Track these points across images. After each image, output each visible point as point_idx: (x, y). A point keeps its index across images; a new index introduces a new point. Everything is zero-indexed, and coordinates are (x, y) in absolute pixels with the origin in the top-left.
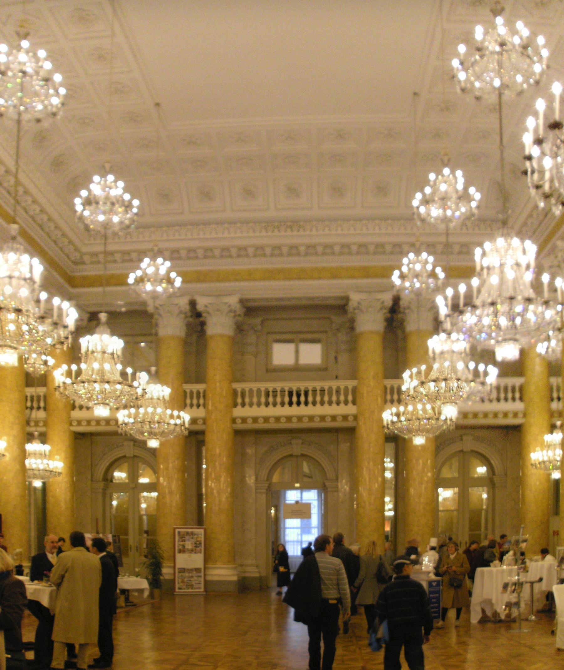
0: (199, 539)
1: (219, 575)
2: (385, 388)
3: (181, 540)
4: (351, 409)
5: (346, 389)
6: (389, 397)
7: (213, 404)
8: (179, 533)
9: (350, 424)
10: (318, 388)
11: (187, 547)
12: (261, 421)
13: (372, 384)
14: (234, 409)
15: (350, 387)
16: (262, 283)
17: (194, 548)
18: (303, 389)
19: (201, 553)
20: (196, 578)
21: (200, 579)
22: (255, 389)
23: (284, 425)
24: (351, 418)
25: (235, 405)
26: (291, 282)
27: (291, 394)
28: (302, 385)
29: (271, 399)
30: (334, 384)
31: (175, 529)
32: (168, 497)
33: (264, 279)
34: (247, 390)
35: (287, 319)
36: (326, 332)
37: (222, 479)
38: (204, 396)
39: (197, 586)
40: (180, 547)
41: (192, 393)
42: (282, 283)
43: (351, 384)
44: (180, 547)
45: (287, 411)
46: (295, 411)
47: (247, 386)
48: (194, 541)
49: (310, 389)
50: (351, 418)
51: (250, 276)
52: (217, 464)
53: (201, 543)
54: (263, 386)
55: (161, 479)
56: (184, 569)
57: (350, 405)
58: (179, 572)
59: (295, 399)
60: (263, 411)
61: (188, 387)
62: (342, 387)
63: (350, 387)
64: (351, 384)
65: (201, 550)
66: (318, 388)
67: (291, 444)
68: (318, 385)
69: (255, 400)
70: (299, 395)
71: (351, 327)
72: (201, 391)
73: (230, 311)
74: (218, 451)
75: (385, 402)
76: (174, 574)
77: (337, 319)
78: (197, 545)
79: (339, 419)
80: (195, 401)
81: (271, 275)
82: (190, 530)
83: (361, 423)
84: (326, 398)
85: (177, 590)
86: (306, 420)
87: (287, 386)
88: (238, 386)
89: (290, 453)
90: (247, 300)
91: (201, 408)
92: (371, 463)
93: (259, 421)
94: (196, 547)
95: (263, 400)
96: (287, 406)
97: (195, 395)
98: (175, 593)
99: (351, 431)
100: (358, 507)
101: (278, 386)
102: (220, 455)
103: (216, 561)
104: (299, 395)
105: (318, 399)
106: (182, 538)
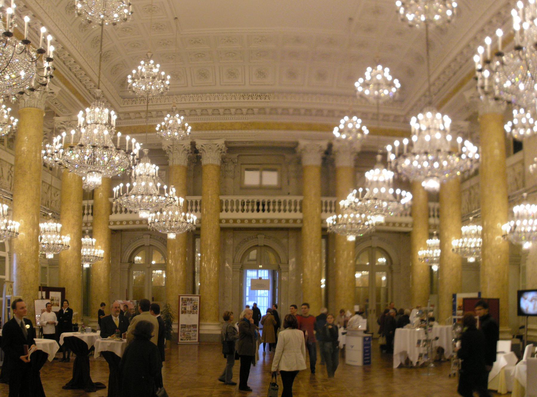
0: (196, 304)
1: (209, 330)
2: (322, 202)
3: (183, 304)
4: (298, 215)
5: (296, 202)
6: (324, 208)
7: (206, 210)
8: (182, 299)
9: (297, 225)
10: (277, 200)
11: (187, 309)
12: (239, 221)
13: (313, 199)
14: (221, 213)
15: (298, 201)
16: (240, 131)
17: (192, 310)
18: (266, 201)
19: (197, 314)
20: (192, 332)
21: (195, 333)
22: (235, 200)
23: (254, 225)
24: (299, 221)
25: (221, 211)
26: (260, 132)
27: (258, 204)
28: (266, 198)
29: (245, 207)
30: (288, 198)
31: (179, 296)
32: (174, 273)
33: (241, 129)
34: (230, 200)
35: (255, 155)
36: (280, 164)
37: (212, 261)
38: (200, 204)
39: (194, 338)
40: (183, 309)
41: (192, 202)
42: (253, 131)
43: (299, 198)
44: (183, 309)
45: (256, 215)
46: (261, 215)
47: (229, 198)
48: (192, 305)
49: (272, 201)
50: (299, 221)
51: (232, 127)
52: (209, 250)
53: (197, 307)
54: (240, 198)
55: (170, 261)
56: (185, 325)
57: (298, 212)
58: (182, 328)
59: (261, 207)
60: (240, 215)
61: (190, 198)
62: (293, 200)
63: (298, 201)
64: (299, 198)
65: (197, 311)
66: (277, 200)
67: (257, 238)
68: (277, 198)
69: (235, 207)
70: (263, 205)
71: (299, 161)
72: (198, 201)
73: (218, 149)
74: (209, 242)
75: (322, 211)
76: (179, 328)
77: (289, 157)
78: (194, 308)
79: (291, 221)
80: (194, 208)
81: (246, 126)
82: (190, 297)
83: (306, 225)
84: (282, 207)
85: (180, 341)
86: (268, 221)
87: (256, 198)
88: (224, 198)
89: (257, 244)
90: (230, 142)
91: (198, 212)
92: (313, 252)
93: (238, 221)
94: (194, 309)
95: (240, 207)
96: (255, 212)
97: (194, 204)
98: (178, 343)
99: (298, 230)
100: (303, 283)
101: (250, 198)
102: (211, 245)
103: (207, 320)
104: (263, 205)
105: (277, 207)
106: (184, 302)
